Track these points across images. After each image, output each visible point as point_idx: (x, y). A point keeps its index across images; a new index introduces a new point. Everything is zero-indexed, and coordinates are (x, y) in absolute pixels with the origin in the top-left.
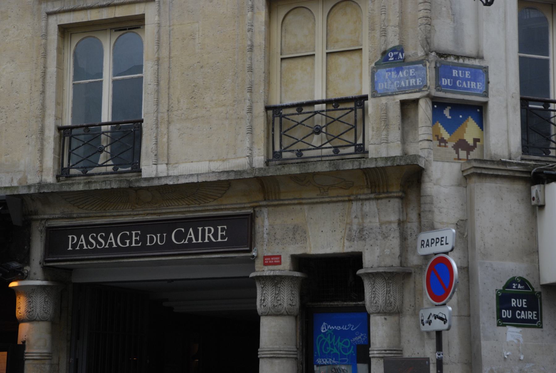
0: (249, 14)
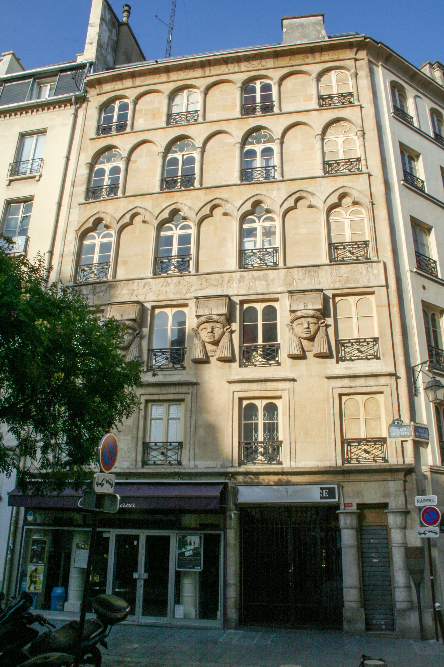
0: (332, 400)
